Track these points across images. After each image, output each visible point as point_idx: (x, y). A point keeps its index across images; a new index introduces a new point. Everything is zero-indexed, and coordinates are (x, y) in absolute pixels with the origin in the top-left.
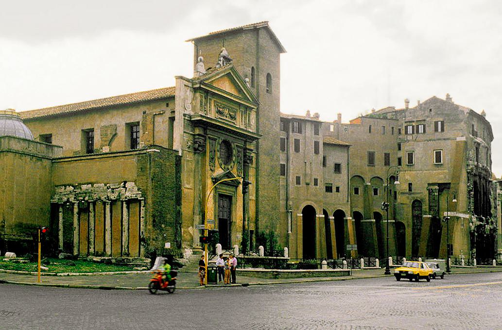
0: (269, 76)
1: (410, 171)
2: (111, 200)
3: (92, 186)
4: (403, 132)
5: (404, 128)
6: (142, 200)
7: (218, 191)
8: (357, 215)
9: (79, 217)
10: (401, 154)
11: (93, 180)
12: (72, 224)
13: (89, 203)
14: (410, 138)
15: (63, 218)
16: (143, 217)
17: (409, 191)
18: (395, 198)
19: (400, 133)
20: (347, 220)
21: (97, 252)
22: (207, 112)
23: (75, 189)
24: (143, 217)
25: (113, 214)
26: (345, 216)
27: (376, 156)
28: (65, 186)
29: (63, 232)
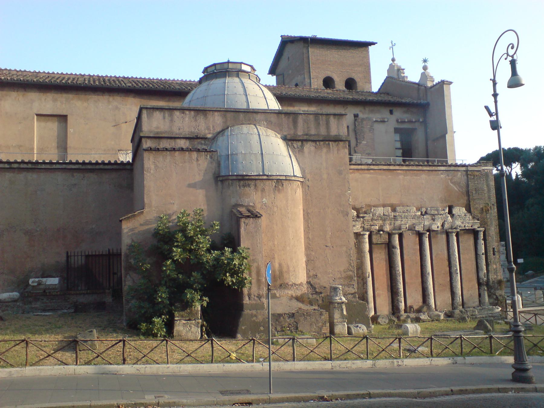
3: (394, 210)
6: (481, 231)
11: (394, 201)
13: (390, 235)
21: (411, 307)
25: (433, 251)
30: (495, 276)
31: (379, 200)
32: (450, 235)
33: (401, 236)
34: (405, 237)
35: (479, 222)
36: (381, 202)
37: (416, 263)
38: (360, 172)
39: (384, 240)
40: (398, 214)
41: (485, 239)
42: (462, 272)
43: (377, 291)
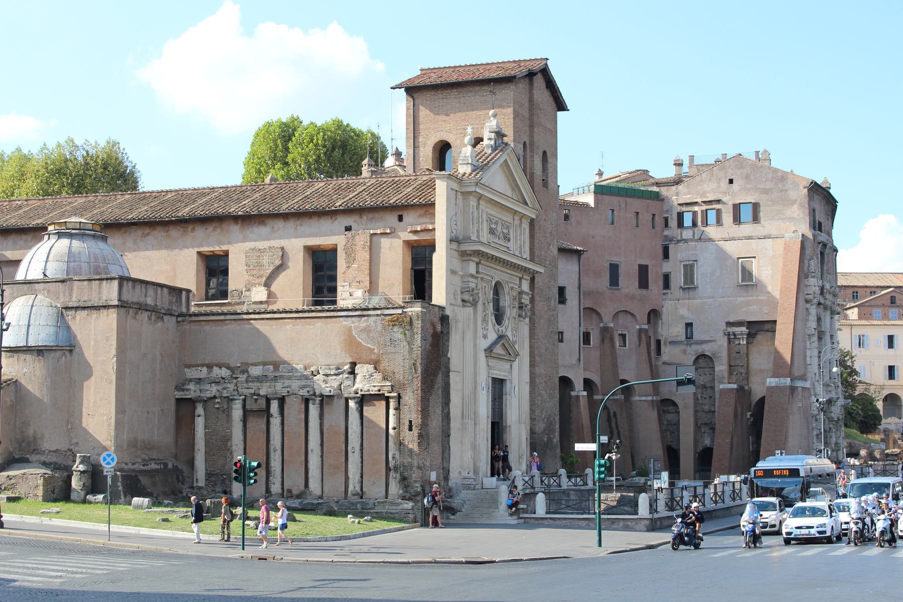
0: (545, 153)
1: (689, 299)
2: (322, 396)
4: (673, 223)
5: (675, 216)
6: (393, 397)
7: (492, 374)
8: (588, 384)
9: (245, 426)
10: (667, 267)
12: (228, 439)
13: (268, 401)
14: (687, 234)
15: (206, 427)
17: (687, 338)
18: (659, 351)
19: (666, 225)
20: (578, 397)
22: (479, 235)
23: (234, 373)
26: (573, 389)
27: (621, 270)
28: (210, 367)
29: (206, 452)
30: (410, 460)
33: (282, 401)
36: (261, 360)
37: (299, 436)
38: (238, 322)
41: (397, 409)
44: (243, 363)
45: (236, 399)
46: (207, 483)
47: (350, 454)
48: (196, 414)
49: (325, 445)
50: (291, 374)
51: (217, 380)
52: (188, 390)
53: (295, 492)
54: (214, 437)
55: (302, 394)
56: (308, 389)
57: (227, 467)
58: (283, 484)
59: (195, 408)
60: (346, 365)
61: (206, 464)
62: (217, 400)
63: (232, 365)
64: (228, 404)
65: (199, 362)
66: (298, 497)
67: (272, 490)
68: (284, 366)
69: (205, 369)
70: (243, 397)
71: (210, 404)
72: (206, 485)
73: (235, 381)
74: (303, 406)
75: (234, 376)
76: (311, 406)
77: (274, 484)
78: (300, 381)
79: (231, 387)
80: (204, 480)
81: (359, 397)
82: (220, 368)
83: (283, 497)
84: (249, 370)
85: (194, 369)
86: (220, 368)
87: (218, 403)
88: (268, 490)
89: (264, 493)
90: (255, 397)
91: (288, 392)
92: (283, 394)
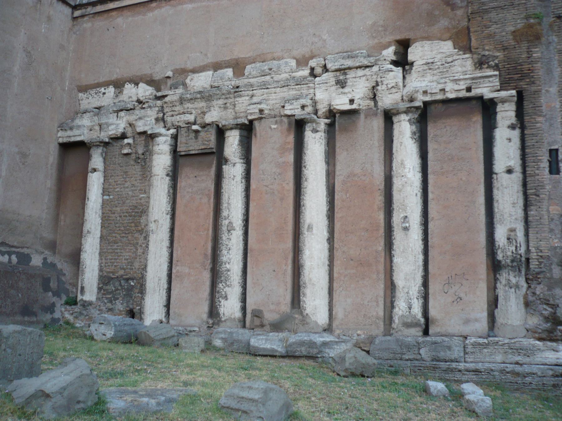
2: (332, 114)
6: (503, 101)
9: (174, 187)
11: (239, 53)
13: (221, 133)
15: (105, 191)
16: (509, 171)
21: (257, 314)
23: (158, 90)
24: (509, 171)
29: (102, 238)
31: (206, 55)
32: (395, 119)
34: (258, 135)
35: (497, 73)
36: (211, 59)
37: (282, 199)
39: (204, 144)
40: (246, 81)
42: (431, 225)
43: (177, 266)
44: (177, 70)
45: (160, 135)
46: (100, 295)
47: (398, 235)
48: (90, 169)
49: (337, 215)
50: (268, 78)
51: (130, 106)
52: (79, 127)
53: (270, 316)
54: (118, 209)
55: (288, 113)
56: (303, 101)
57: (137, 265)
58: (244, 300)
59: (89, 158)
60: (386, 47)
61: (101, 259)
62: (126, 141)
63: (157, 77)
64: (147, 146)
65: (102, 80)
66: (277, 327)
67: (221, 310)
68: (253, 65)
69: (111, 90)
70: (172, 131)
71: (115, 148)
72: (98, 299)
73: (159, 103)
74: (291, 138)
75: (159, 94)
76: (309, 135)
77: (226, 298)
78: (285, 89)
79: (152, 114)
80: (95, 290)
81: (417, 108)
82: (137, 84)
83: (244, 326)
84: (188, 81)
85: (93, 92)
86: (137, 84)
87: (129, 144)
88: (213, 312)
89: (205, 316)
90: (195, 127)
91: (261, 111)
92: (250, 118)
